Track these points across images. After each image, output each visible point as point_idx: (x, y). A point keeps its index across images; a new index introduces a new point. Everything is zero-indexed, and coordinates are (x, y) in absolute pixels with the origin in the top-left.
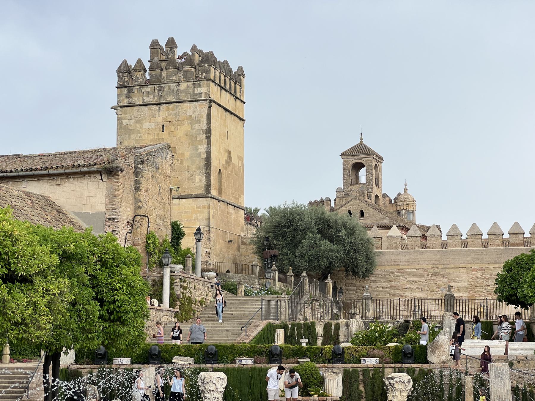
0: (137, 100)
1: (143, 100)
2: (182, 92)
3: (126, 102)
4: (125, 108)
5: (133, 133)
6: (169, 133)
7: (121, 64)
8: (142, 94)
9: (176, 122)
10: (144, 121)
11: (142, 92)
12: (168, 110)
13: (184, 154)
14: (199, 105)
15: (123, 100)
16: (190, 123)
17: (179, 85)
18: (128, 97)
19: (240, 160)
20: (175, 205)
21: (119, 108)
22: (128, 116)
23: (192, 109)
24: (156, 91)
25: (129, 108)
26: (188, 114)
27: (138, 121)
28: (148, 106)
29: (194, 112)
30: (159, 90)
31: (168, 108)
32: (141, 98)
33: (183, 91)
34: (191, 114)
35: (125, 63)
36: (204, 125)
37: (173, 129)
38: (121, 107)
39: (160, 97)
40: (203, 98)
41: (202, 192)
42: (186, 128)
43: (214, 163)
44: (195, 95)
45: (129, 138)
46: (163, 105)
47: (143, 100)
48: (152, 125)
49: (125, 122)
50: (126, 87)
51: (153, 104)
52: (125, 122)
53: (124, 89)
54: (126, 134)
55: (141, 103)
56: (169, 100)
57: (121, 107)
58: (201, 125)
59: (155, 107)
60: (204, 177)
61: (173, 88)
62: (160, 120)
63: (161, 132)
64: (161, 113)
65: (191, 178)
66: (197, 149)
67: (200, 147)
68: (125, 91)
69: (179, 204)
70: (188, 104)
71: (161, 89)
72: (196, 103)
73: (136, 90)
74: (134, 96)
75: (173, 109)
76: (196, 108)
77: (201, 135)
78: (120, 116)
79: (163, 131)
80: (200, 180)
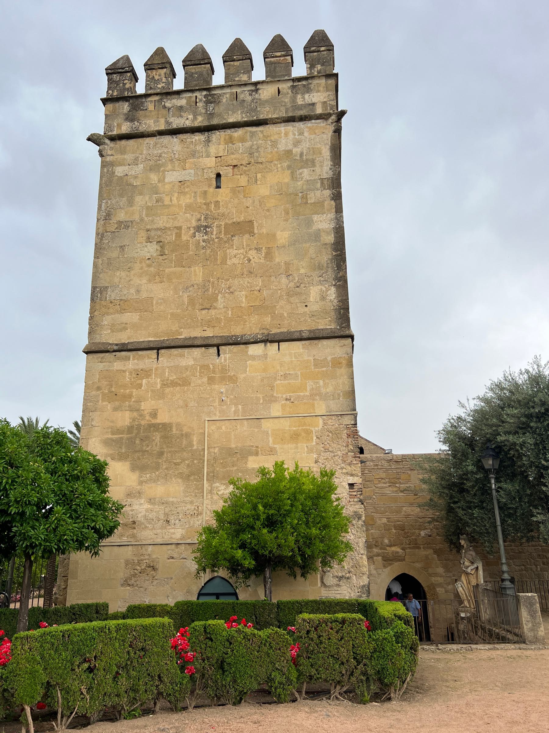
2: (263, 103)
4: (124, 142)
5: (141, 194)
6: (234, 191)
7: (118, 60)
8: (165, 112)
9: (252, 164)
10: (170, 167)
11: (164, 107)
12: (231, 140)
13: (274, 235)
14: (310, 128)
15: (119, 126)
16: (289, 167)
17: (257, 90)
20: (253, 358)
21: (107, 141)
22: (129, 157)
23: (291, 136)
24: (200, 105)
25: (131, 142)
26: (282, 147)
27: (156, 167)
28: (181, 136)
29: (297, 143)
30: (208, 102)
31: (231, 137)
32: (162, 121)
33: (267, 101)
34: (290, 147)
36: (325, 169)
37: (243, 180)
38: (113, 139)
42: (279, 176)
45: (131, 203)
46: (217, 133)
47: (167, 123)
48: (188, 174)
49: (119, 171)
53: (121, 103)
54: (121, 196)
55: (162, 127)
56: (231, 120)
57: (113, 139)
58: (318, 169)
59: (198, 137)
60: (333, 289)
61: (241, 97)
63: (212, 190)
64: (213, 149)
66: (309, 223)
67: (315, 218)
69: (265, 356)
70: (282, 128)
72: (301, 125)
74: (145, 116)
75: (242, 140)
76: (301, 133)
77: (318, 193)
78: (108, 159)
79: (218, 187)
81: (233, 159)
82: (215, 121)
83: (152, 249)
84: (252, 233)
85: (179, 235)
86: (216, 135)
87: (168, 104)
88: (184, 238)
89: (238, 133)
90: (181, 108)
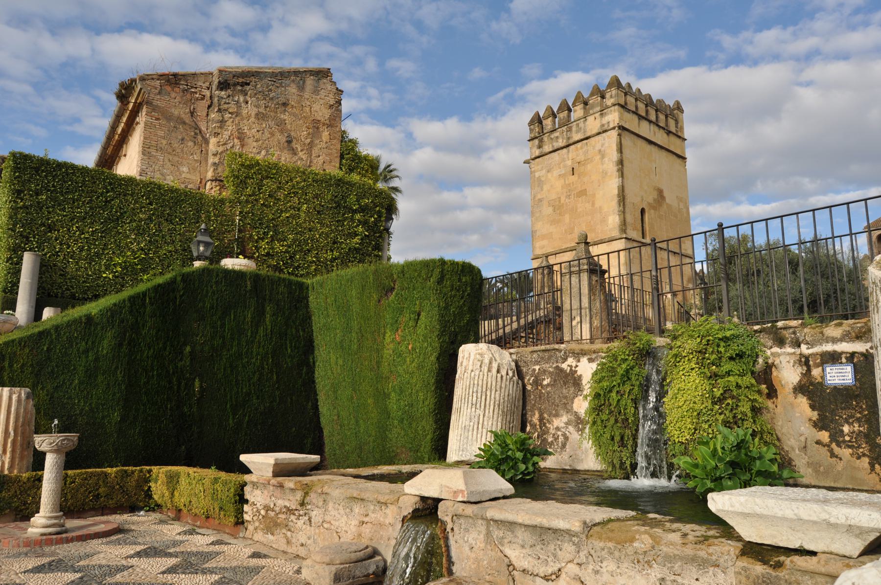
0: (547, 148)
3: (537, 152)
18: (540, 147)
22: (539, 167)
29: (603, 145)
35: (537, 114)
39: (569, 138)
40: (611, 126)
41: (616, 233)
43: (630, 198)
44: (603, 125)
50: (536, 138)
51: (562, 148)
52: (537, 175)
59: (565, 150)
62: (569, 163)
64: (570, 156)
65: (604, 220)
68: (536, 142)
71: (570, 130)
72: (604, 135)
73: (545, 138)
75: (582, 148)
80: (614, 220)
81: (578, 159)
82: (571, 141)
83: (551, 209)
84: (586, 195)
85: (560, 201)
88: (562, 202)
89: (579, 145)
90: (557, 137)
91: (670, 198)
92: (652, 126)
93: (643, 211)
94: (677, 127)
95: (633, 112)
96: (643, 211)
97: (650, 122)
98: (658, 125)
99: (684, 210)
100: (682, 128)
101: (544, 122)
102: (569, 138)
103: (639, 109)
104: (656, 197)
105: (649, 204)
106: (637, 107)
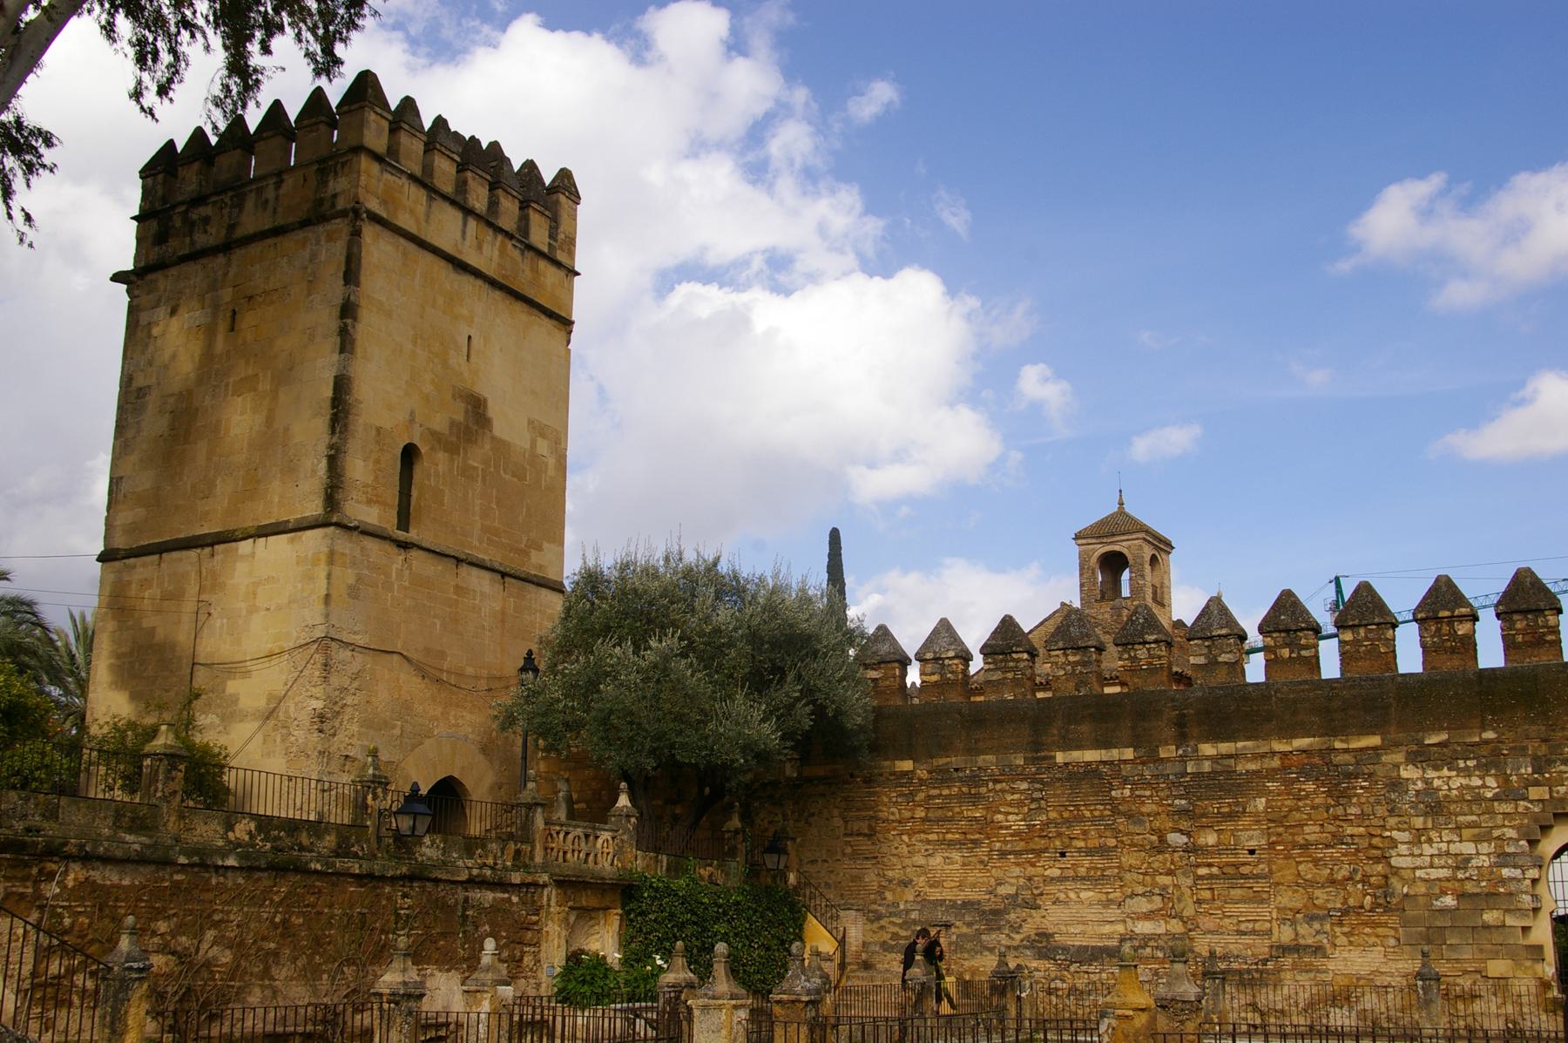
1: (193, 243)
19: (543, 436)
28: (204, 261)
32: (187, 240)
86: (238, 254)
87: (194, 217)
91: (509, 423)
92: (472, 224)
93: (410, 454)
94: (553, 235)
95: (412, 177)
96: (410, 454)
97: (468, 212)
98: (490, 225)
99: (551, 461)
100: (571, 241)
101: (182, 172)
102: (232, 227)
103: (437, 174)
104: (460, 417)
105: (434, 434)
106: (428, 168)
